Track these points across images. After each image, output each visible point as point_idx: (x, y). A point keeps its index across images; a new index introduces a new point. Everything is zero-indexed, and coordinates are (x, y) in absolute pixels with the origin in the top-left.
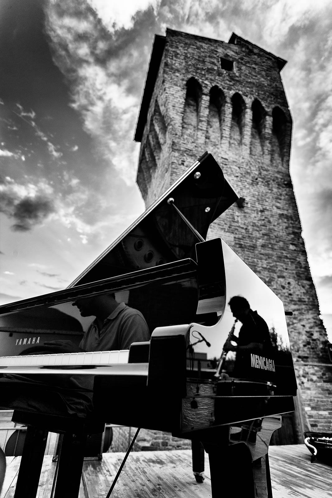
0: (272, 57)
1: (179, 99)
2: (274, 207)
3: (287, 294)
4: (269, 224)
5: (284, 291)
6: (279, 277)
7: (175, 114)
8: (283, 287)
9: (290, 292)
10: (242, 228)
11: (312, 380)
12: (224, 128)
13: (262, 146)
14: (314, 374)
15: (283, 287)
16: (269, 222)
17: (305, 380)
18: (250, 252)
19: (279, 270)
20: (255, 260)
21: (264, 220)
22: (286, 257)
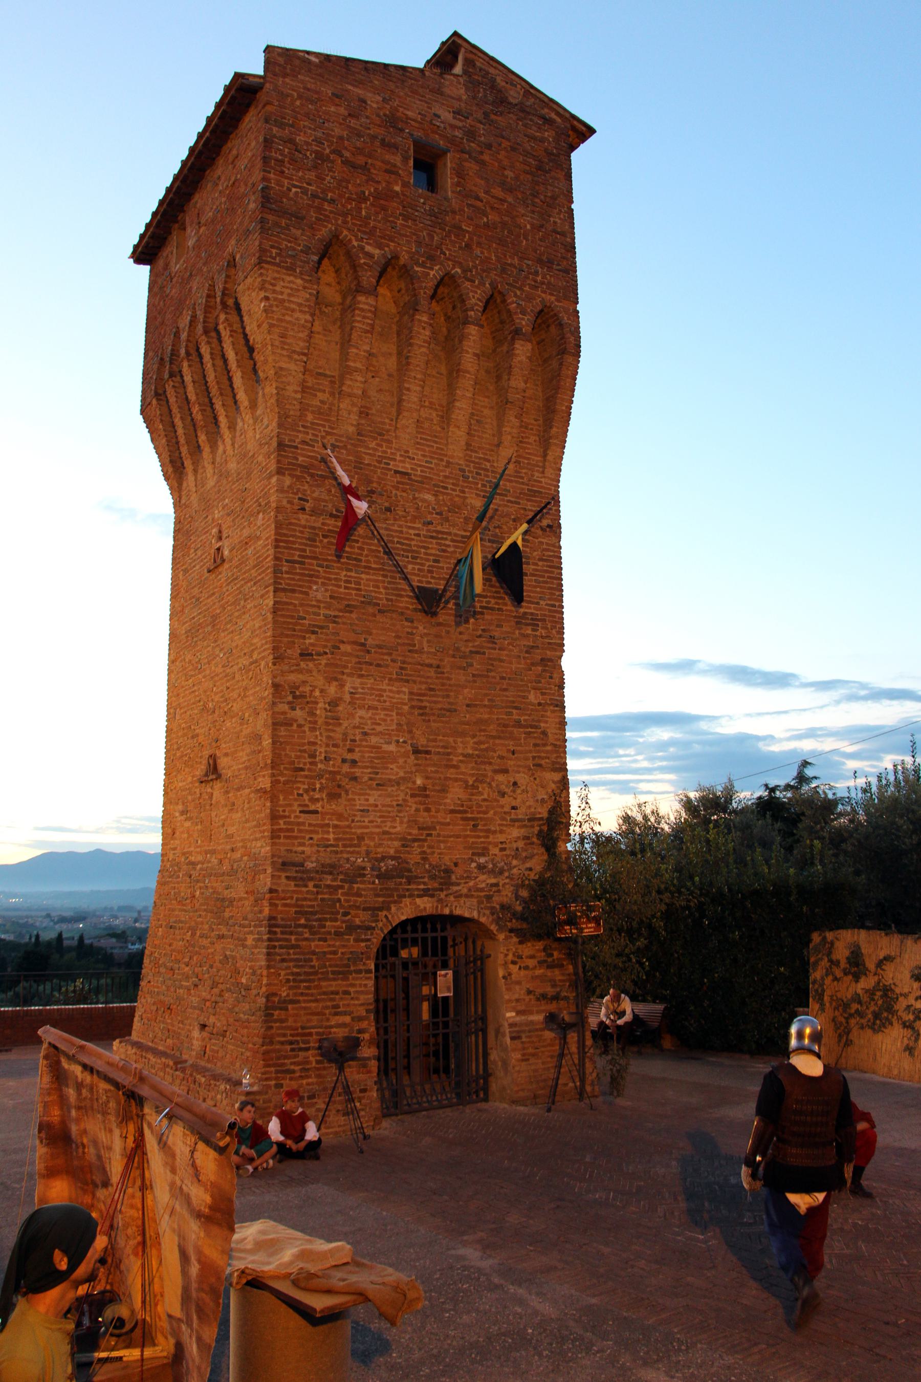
0: (558, 114)
1: (297, 315)
3: (507, 809)
4: (491, 645)
5: (503, 801)
6: (496, 772)
7: (286, 359)
8: (503, 794)
10: (430, 666)
12: (406, 385)
13: (500, 419)
14: (532, 957)
15: (503, 794)
17: (514, 969)
18: (443, 722)
20: (451, 740)
21: (480, 636)
22: (518, 724)
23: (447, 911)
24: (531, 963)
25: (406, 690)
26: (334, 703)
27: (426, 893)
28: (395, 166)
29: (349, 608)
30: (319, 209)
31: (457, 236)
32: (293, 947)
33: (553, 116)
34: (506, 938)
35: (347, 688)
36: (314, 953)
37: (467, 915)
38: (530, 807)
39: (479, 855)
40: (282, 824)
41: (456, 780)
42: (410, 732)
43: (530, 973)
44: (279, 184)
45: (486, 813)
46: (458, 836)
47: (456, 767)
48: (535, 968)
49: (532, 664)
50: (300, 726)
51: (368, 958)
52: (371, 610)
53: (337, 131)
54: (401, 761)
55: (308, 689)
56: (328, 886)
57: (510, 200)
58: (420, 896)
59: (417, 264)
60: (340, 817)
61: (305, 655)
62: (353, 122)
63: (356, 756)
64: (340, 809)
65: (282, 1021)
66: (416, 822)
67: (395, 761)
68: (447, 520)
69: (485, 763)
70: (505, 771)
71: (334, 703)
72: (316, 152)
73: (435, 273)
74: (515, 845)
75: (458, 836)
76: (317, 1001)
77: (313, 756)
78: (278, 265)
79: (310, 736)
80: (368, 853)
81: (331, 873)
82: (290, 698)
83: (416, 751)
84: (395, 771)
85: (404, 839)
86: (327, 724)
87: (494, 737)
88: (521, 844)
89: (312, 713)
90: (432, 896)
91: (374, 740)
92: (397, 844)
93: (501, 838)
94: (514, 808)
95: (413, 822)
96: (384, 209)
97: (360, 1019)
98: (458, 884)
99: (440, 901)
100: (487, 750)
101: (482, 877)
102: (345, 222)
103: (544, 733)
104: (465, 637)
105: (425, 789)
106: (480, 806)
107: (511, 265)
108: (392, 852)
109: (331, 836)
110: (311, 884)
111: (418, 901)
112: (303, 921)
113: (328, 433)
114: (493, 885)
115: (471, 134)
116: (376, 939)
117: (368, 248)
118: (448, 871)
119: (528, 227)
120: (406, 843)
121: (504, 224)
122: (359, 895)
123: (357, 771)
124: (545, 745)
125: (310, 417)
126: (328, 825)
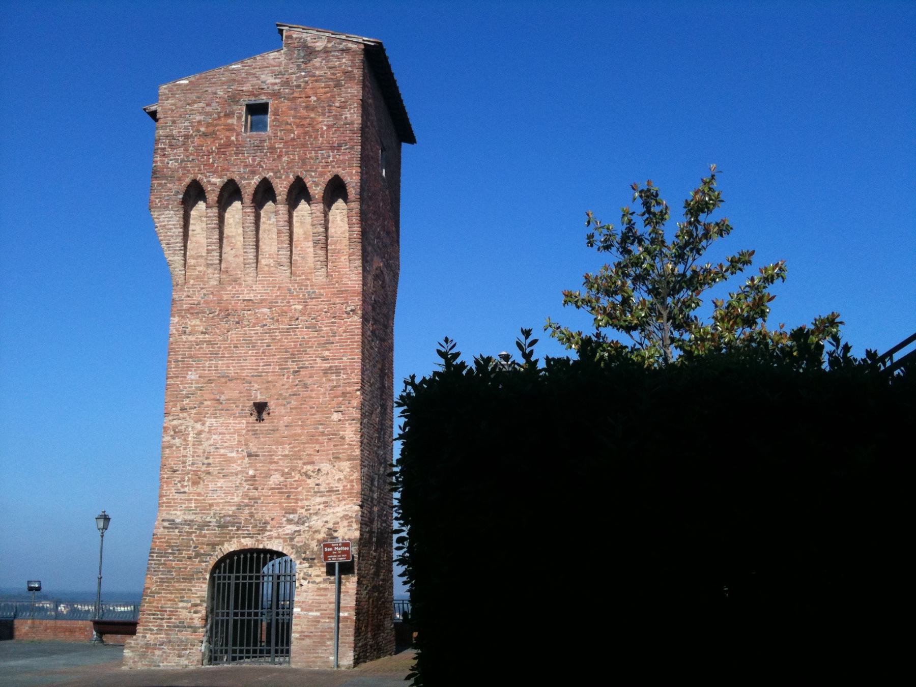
2: (318, 360)
3: (313, 485)
5: (309, 481)
6: (304, 464)
9: (317, 482)
11: (314, 582)
14: (318, 576)
15: (309, 477)
16: (306, 386)
19: (307, 455)
20: (274, 447)
22: (323, 434)
23: (261, 547)
24: (318, 580)
25: (244, 422)
26: (200, 433)
27: (250, 536)
28: (233, 124)
29: (210, 381)
30: (184, 168)
31: (271, 153)
32: (161, 564)
33: (350, 45)
34: (300, 564)
35: (207, 424)
36: (173, 568)
37: (275, 549)
38: (329, 484)
39: (290, 513)
40: (164, 499)
41: (276, 470)
42: (246, 445)
43: (317, 586)
44: (162, 162)
45: (296, 488)
46: (275, 503)
47: (275, 462)
48: (320, 583)
49: (335, 397)
50: (177, 447)
51: (206, 571)
52: (223, 380)
53: (198, 118)
54: (239, 462)
55: (183, 427)
56: (187, 532)
57: (312, 115)
58: (244, 537)
59: (243, 178)
60: (199, 494)
61: (183, 409)
62: (208, 109)
63: (210, 461)
64: (199, 490)
65: (150, 603)
66: (247, 495)
67: (235, 462)
68: (278, 321)
69: (296, 459)
70: (313, 463)
71: (200, 433)
72: (185, 136)
73: (256, 180)
74: (318, 507)
75: (275, 503)
76: (172, 593)
77: (184, 462)
78: (159, 207)
79: (183, 452)
80: (215, 514)
81: (189, 525)
82: (172, 433)
83: (250, 455)
84: (235, 467)
85: (240, 505)
86: (194, 445)
87: (304, 443)
88: (321, 506)
89: (185, 440)
90: (252, 537)
91: (222, 451)
92: (234, 508)
93: (306, 503)
94: (317, 485)
95: (245, 495)
96: (224, 153)
97: (196, 605)
98: (271, 531)
99: (258, 541)
100: (299, 451)
101: (289, 527)
102: (200, 170)
103: (343, 438)
104: (286, 387)
105: (254, 476)
106: (291, 484)
107: (311, 158)
108: (231, 513)
109: (193, 505)
110: (177, 531)
111: (242, 540)
112: (170, 551)
113: (202, 288)
114: (295, 531)
115: (286, 83)
116: (212, 561)
117: (214, 180)
118: (266, 523)
119: (325, 128)
120: (239, 507)
121: (306, 133)
122: (205, 536)
123: (211, 469)
124: (342, 445)
125: (192, 282)
126: (191, 500)
